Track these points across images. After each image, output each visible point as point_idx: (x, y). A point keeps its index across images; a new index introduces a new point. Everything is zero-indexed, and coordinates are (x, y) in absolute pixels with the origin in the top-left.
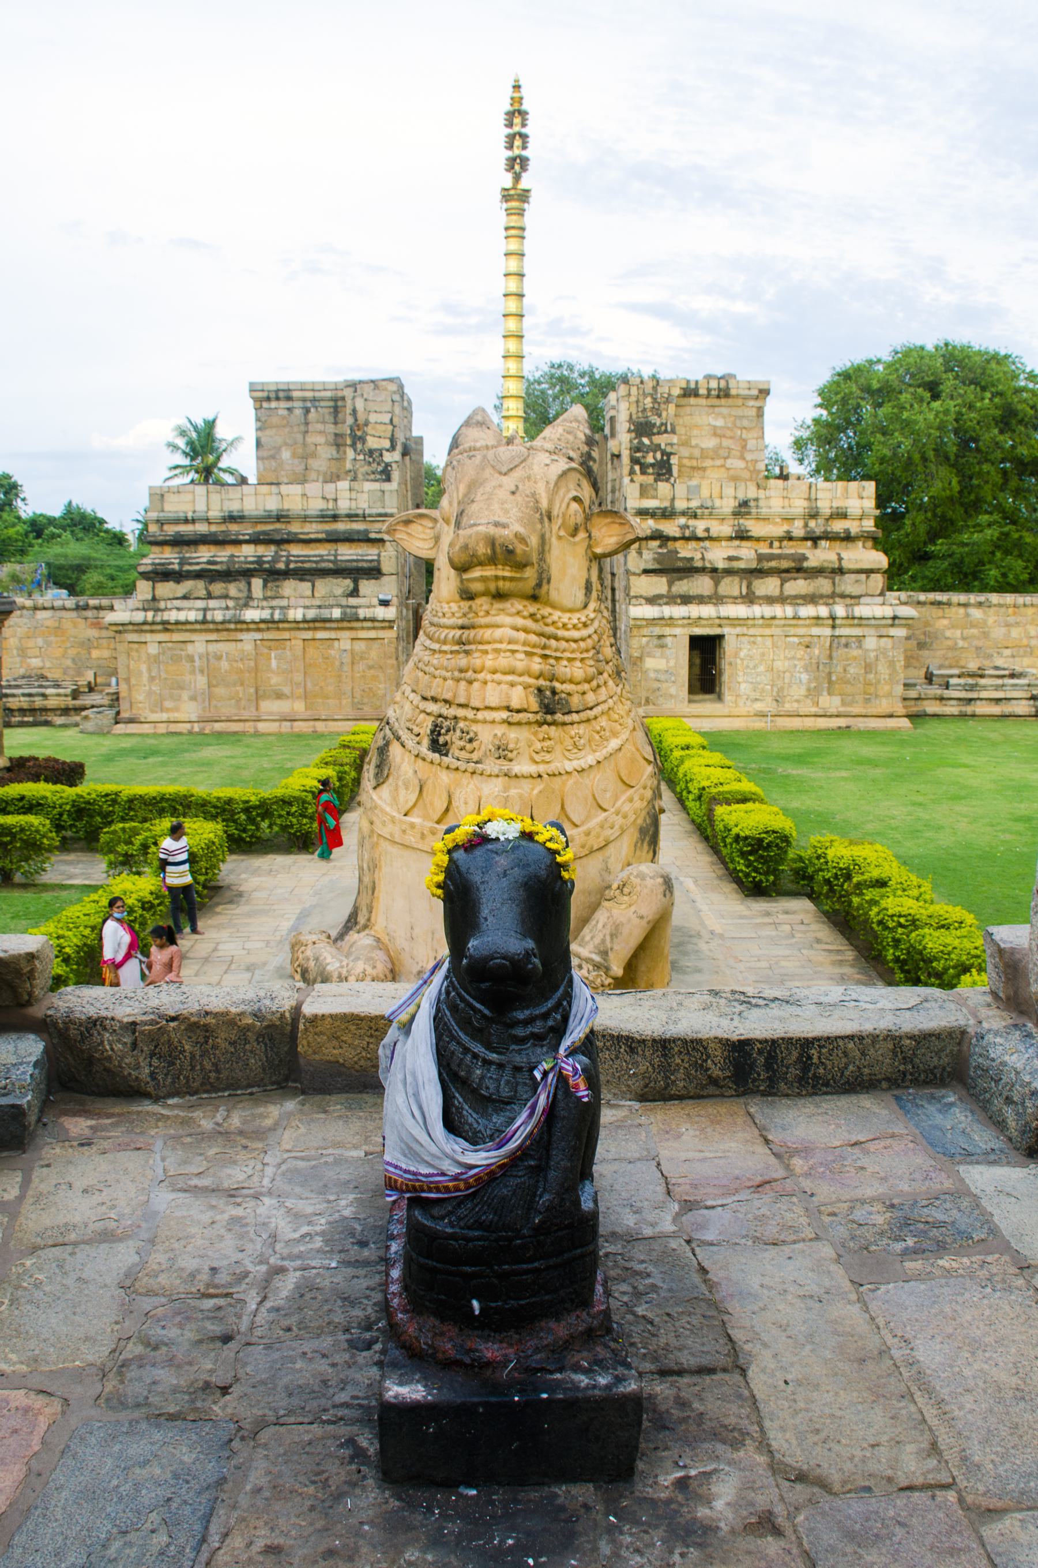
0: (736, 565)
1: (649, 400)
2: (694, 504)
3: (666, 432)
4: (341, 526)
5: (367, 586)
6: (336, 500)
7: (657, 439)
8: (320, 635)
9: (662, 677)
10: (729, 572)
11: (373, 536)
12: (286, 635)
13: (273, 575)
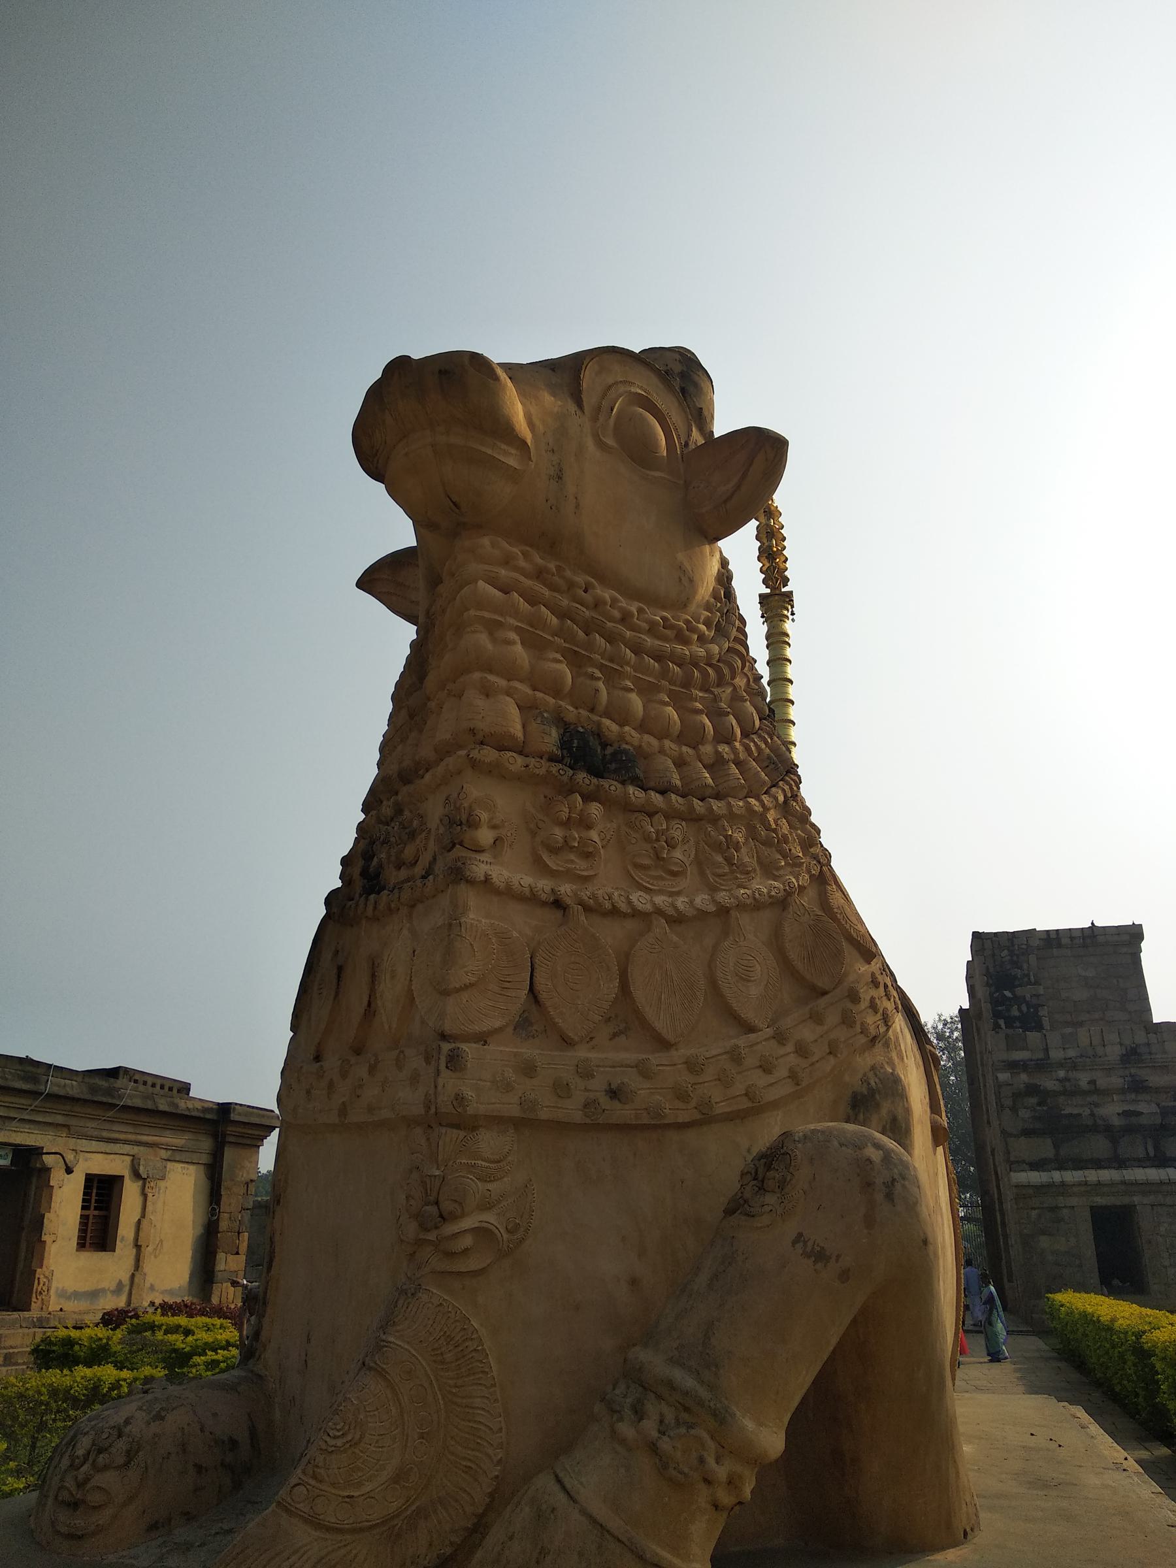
1: (1006, 952)
2: (1071, 1053)
3: (1030, 983)
7: (1019, 991)
10: (1128, 1130)
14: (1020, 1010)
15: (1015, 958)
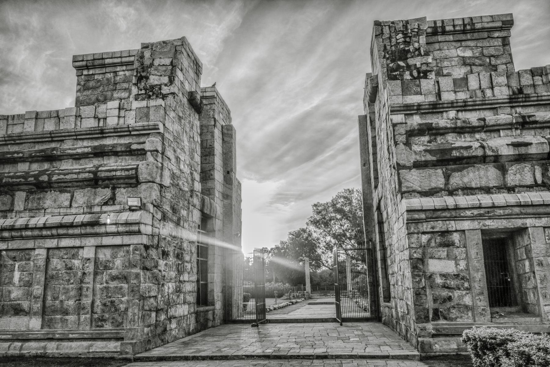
0: (523, 150)
1: (400, 35)
2: (462, 96)
3: (420, 55)
4: (108, 142)
5: (122, 194)
6: (105, 119)
8: (65, 243)
9: (452, 283)
11: (134, 147)
12: (30, 244)
13: (39, 187)
14: (411, 75)
15: (408, 39)
